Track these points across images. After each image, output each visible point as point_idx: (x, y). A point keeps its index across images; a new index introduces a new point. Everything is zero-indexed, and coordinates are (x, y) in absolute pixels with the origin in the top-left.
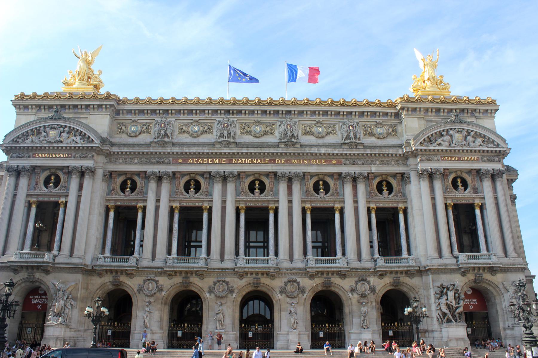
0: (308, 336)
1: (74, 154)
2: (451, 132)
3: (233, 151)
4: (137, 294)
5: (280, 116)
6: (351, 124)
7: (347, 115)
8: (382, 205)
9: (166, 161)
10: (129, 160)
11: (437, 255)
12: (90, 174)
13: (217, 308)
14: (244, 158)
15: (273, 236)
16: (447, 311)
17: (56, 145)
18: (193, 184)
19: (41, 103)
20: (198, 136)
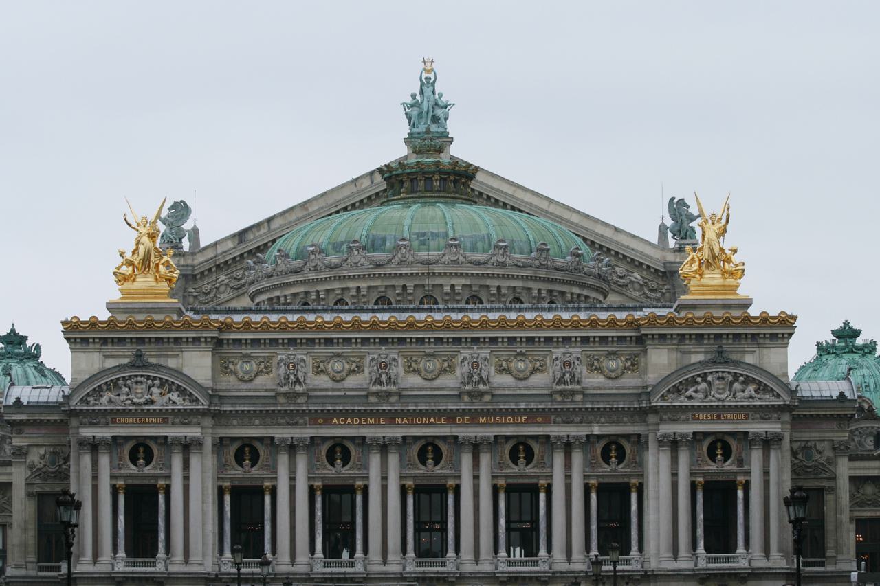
1: (171, 418)
2: (710, 378)
5: (463, 345)
6: (567, 359)
7: (563, 342)
9: (301, 421)
10: (246, 420)
15: (453, 526)
18: (339, 451)
20: (343, 380)
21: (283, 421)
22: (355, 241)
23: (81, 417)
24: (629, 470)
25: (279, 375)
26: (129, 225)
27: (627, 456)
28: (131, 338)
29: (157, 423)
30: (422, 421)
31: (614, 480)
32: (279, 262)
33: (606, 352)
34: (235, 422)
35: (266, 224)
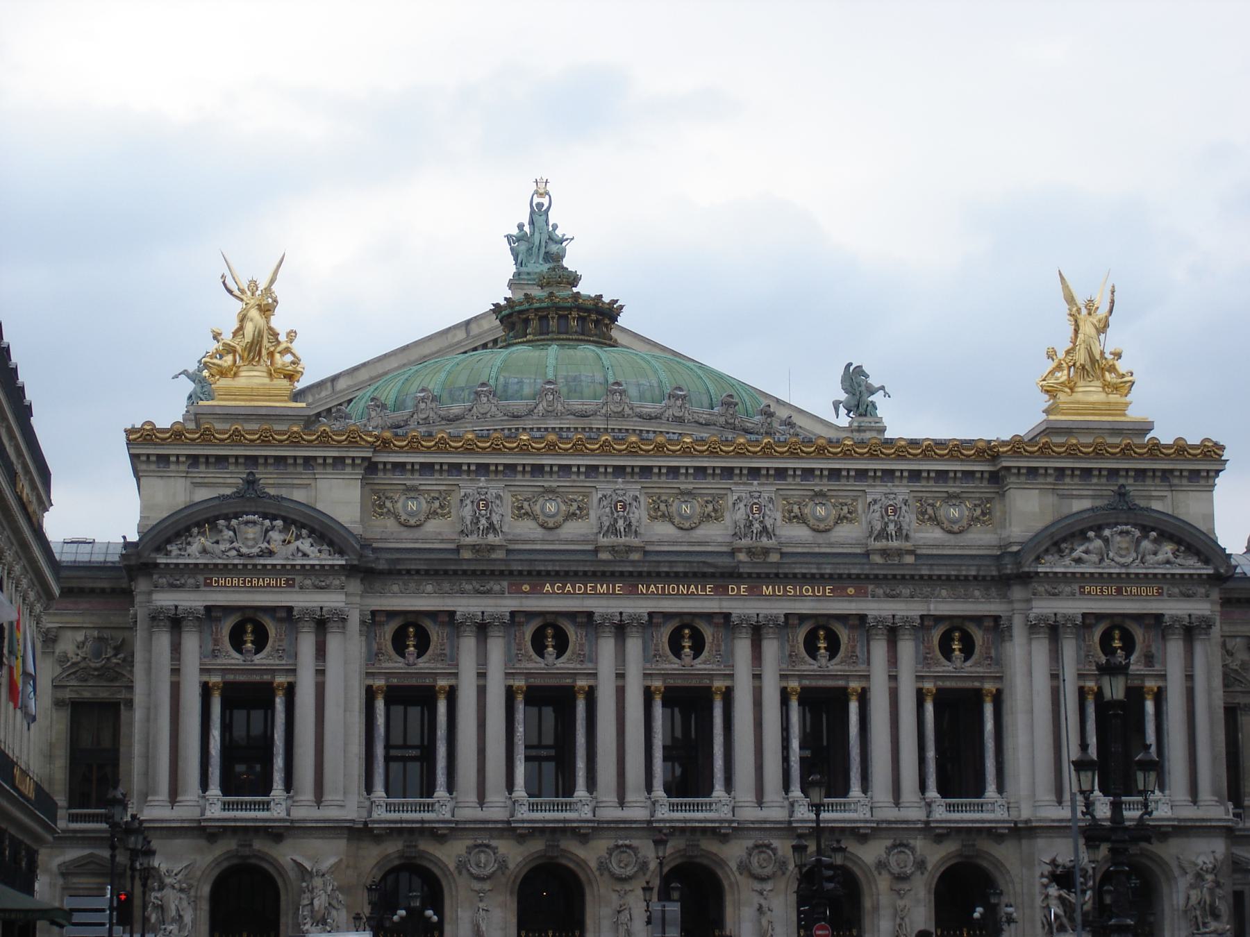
1: (298, 579)
5: (736, 479)
7: (881, 478)
17: (262, 562)
18: (550, 633)
19: (201, 452)
21: (468, 587)
22: (483, 384)
23: (155, 577)
24: (981, 669)
25: (463, 518)
26: (230, 292)
27: (977, 650)
28: (237, 457)
31: (961, 685)
32: (373, 414)
34: (395, 588)
35: (329, 384)
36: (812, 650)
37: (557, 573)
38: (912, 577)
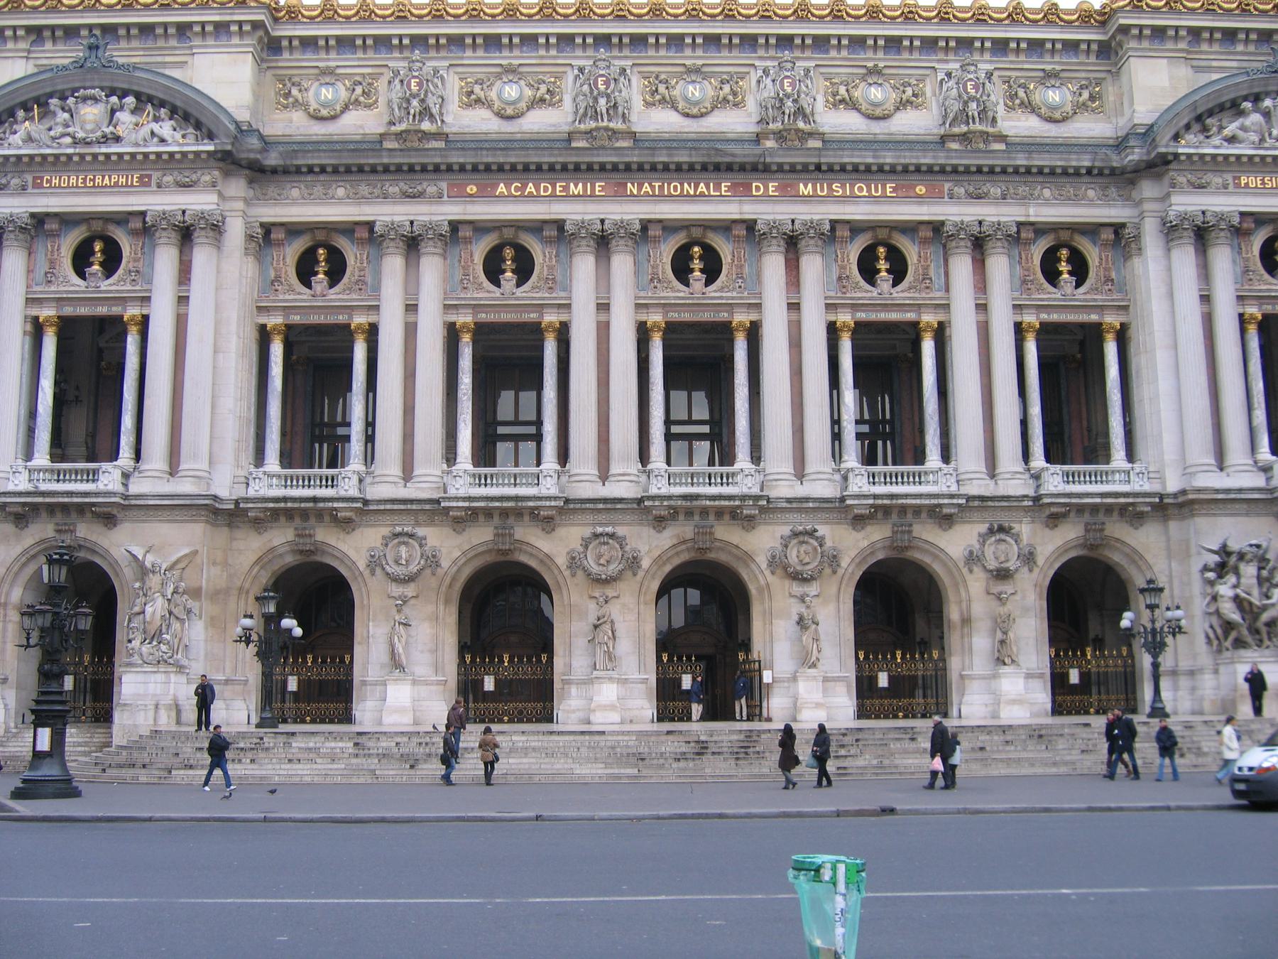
0: (849, 687)
1: (156, 176)
3: (627, 159)
4: (367, 573)
5: (761, 52)
7: (956, 50)
8: (1055, 317)
11: (1213, 462)
12: (211, 234)
13: (592, 610)
14: (657, 180)
16: (1236, 617)
17: (104, 150)
18: (509, 255)
21: (393, 190)
27: (1092, 274)
29: (127, 186)
30: (682, 189)
33: (1041, 74)
34: (295, 193)
36: (868, 272)
37: (513, 168)
38: (1004, 171)
